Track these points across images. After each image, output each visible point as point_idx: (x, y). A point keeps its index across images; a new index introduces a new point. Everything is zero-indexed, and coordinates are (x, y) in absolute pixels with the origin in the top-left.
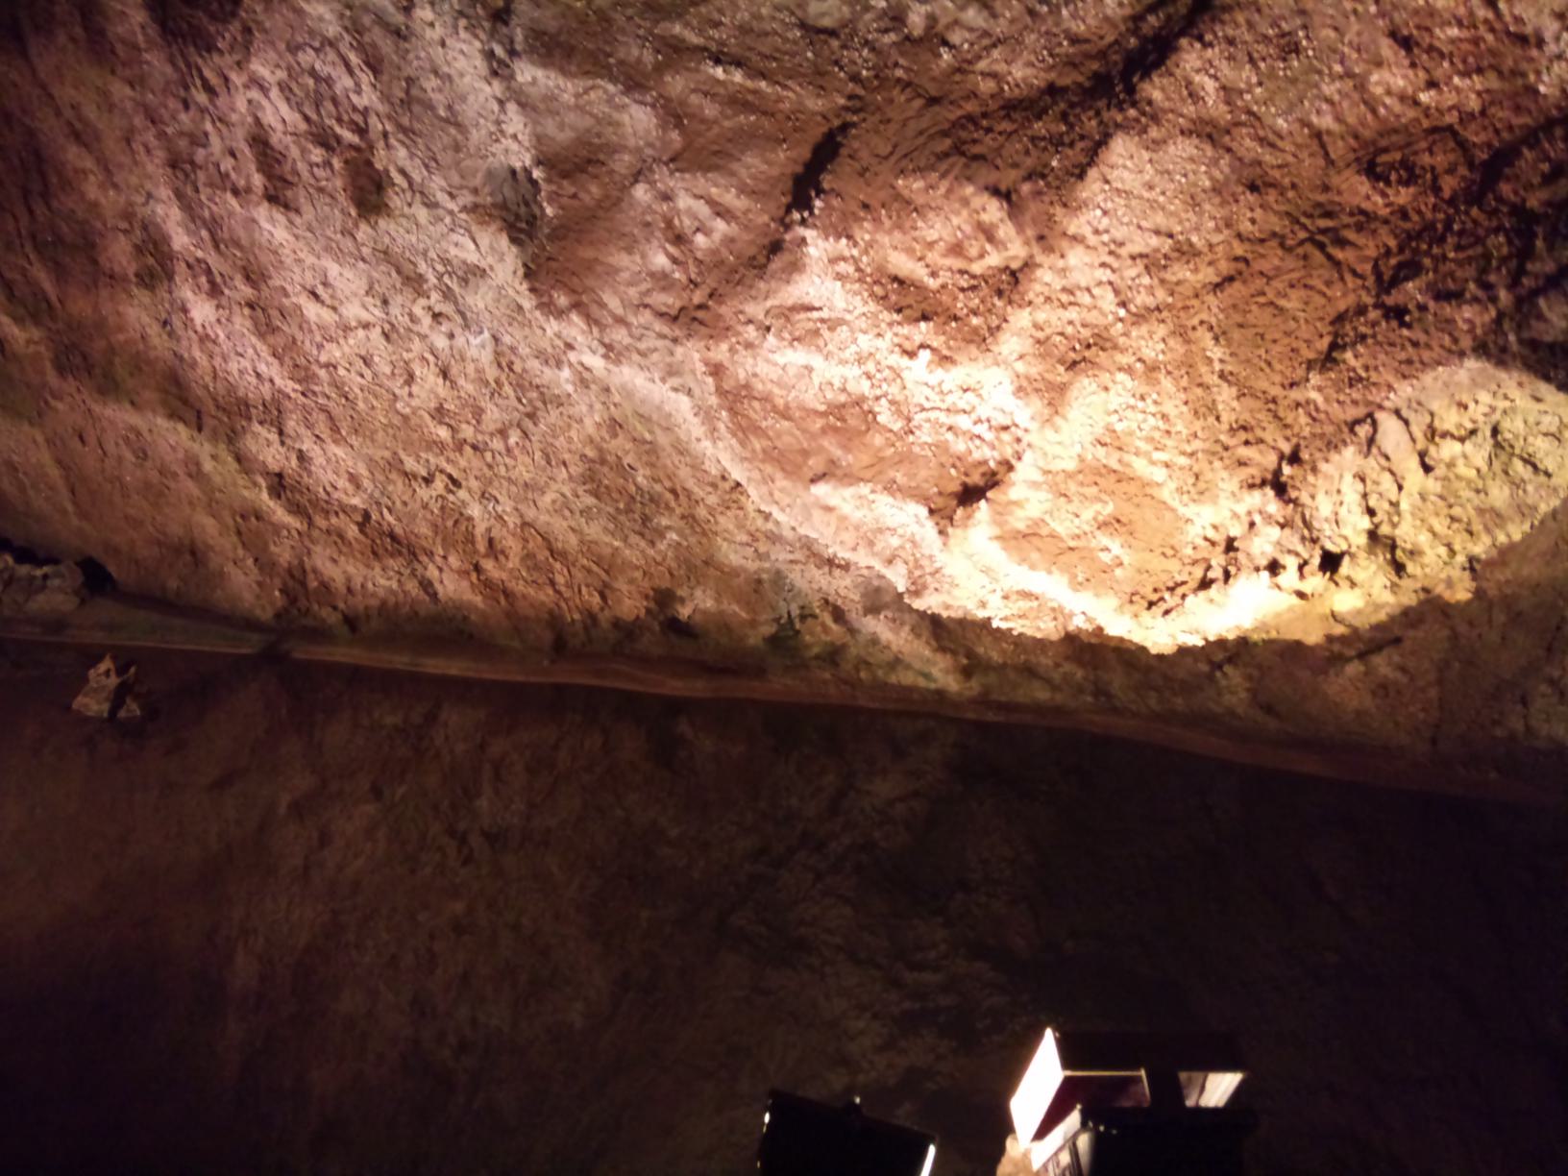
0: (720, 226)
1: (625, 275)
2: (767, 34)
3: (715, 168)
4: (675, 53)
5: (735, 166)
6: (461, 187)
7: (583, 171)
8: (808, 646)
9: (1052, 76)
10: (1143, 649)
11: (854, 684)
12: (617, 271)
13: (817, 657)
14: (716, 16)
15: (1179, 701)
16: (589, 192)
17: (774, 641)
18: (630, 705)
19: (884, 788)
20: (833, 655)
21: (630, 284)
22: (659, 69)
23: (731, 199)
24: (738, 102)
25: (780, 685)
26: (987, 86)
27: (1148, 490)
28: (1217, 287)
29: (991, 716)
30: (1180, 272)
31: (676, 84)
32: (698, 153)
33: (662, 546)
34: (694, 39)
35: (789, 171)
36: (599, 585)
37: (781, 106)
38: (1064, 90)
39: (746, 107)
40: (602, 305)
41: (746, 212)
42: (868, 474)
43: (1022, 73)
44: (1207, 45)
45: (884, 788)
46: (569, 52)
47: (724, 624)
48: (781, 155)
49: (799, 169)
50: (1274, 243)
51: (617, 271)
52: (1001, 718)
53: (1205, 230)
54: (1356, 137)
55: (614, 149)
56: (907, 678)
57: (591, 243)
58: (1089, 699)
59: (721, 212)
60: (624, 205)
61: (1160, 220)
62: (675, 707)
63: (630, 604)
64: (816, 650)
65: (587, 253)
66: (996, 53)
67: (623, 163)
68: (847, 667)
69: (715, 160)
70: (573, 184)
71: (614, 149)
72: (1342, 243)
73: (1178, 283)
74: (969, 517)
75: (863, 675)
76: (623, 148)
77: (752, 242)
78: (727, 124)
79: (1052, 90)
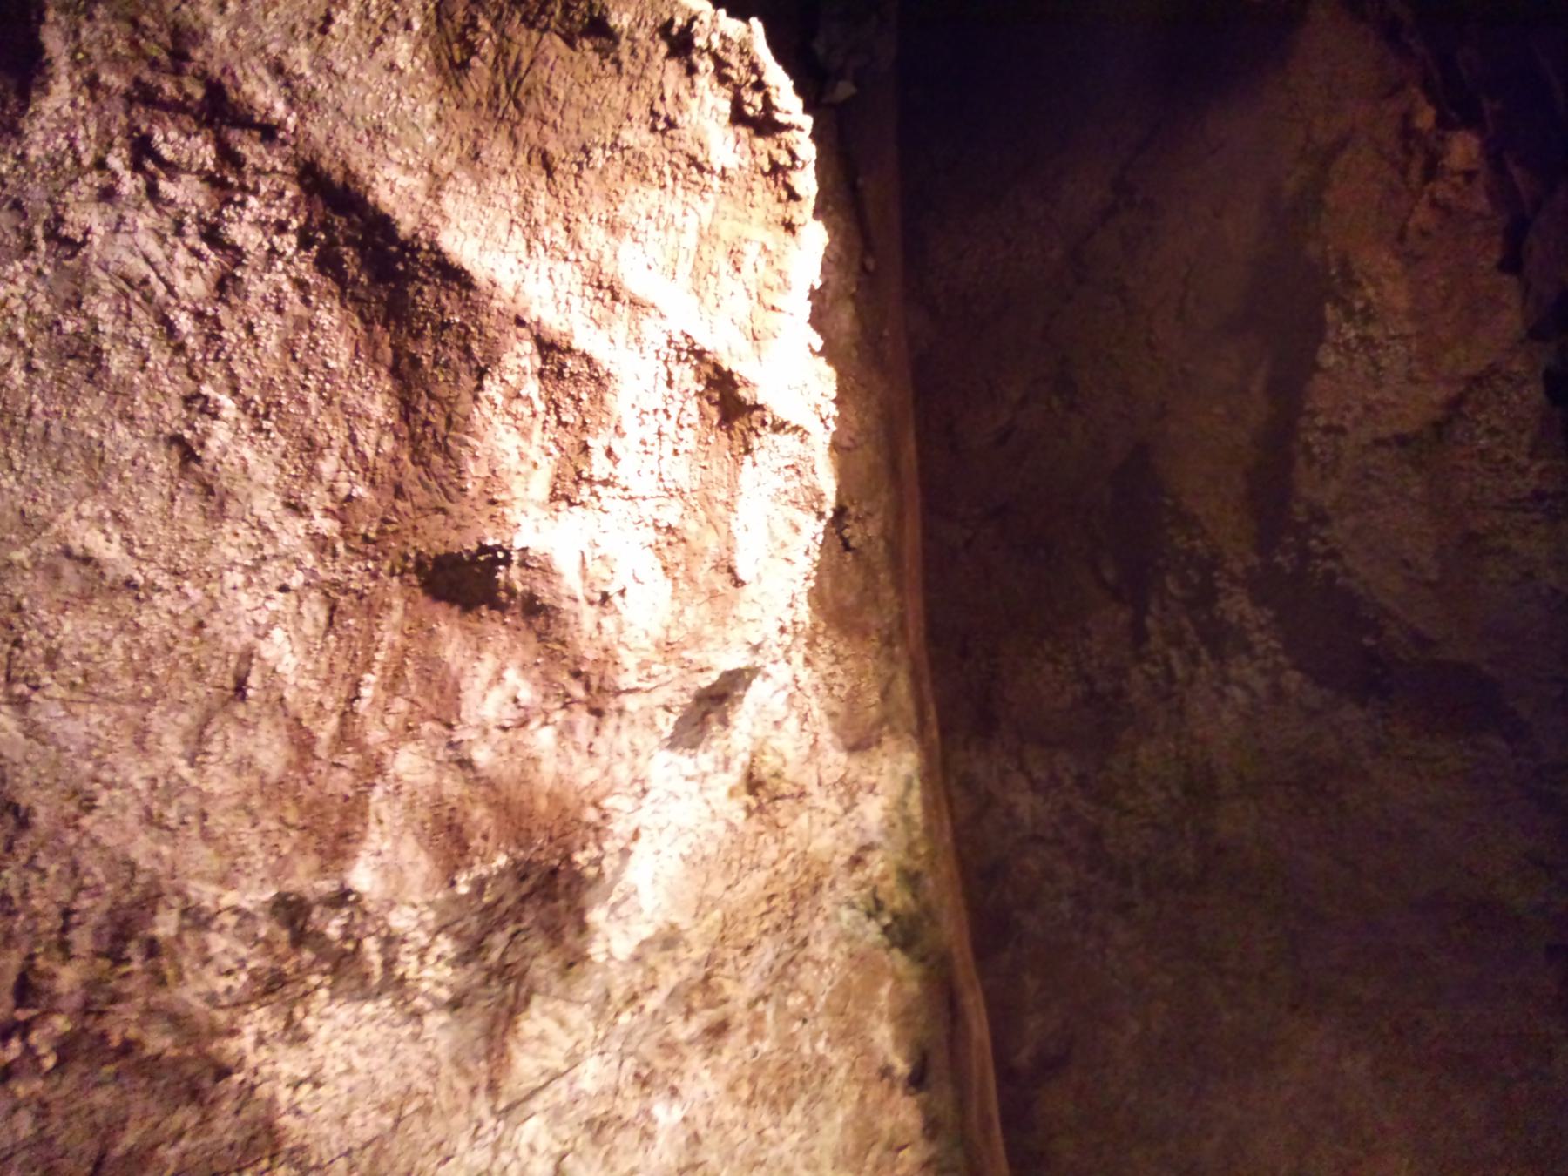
0: (511, 675)
1: (563, 768)
2: (331, 665)
3: (457, 684)
4: (346, 737)
5: (454, 668)
6: (469, 1111)
7: (460, 829)
8: (905, 905)
9: (383, 371)
10: (828, 248)
11: (932, 854)
12: (558, 775)
13: (914, 896)
14: (313, 706)
15: (882, 576)
16: (482, 819)
17: (905, 946)
18: (1017, 1117)
19: (1026, 804)
20: (910, 879)
21: (570, 763)
22: (361, 748)
23: (487, 666)
24: (392, 685)
25: (951, 930)
26: (388, 445)
27: (705, 231)
28: (550, 175)
29: (932, 717)
30: (539, 213)
31: (375, 735)
32: (444, 700)
33: (833, 1058)
34: (333, 723)
35: (456, 620)
36: (888, 1156)
37: (398, 644)
38: (397, 350)
39: (399, 674)
40: (593, 784)
41: (497, 655)
42: (723, 528)
43: (379, 407)
44: (373, 179)
45: (1026, 804)
46: (344, 836)
47: (903, 1018)
48: (444, 628)
49: (456, 610)
50: (517, 130)
51: (558, 775)
52: (932, 708)
53: (507, 189)
54: (440, 90)
55: (439, 801)
56: (916, 809)
57: (532, 801)
58: (897, 649)
59: (498, 678)
60: (493, 775)
61: (502, 227)
62: (1007, 1074)
63: (904, 1114)
64: (908, 898)
65: (542, 804)
66: (360, 438)
67: (453, 786)
68: (917, 865)
69: (448, 690)
70: (473, 836)
71: (439, 801)
72: (518, 63)
73: (548, 212)
74: (746, 384)
75: (922, 850)
76: (438, 785)
77: (524, 643)
78: (413, 687)
79: (395, 372)
